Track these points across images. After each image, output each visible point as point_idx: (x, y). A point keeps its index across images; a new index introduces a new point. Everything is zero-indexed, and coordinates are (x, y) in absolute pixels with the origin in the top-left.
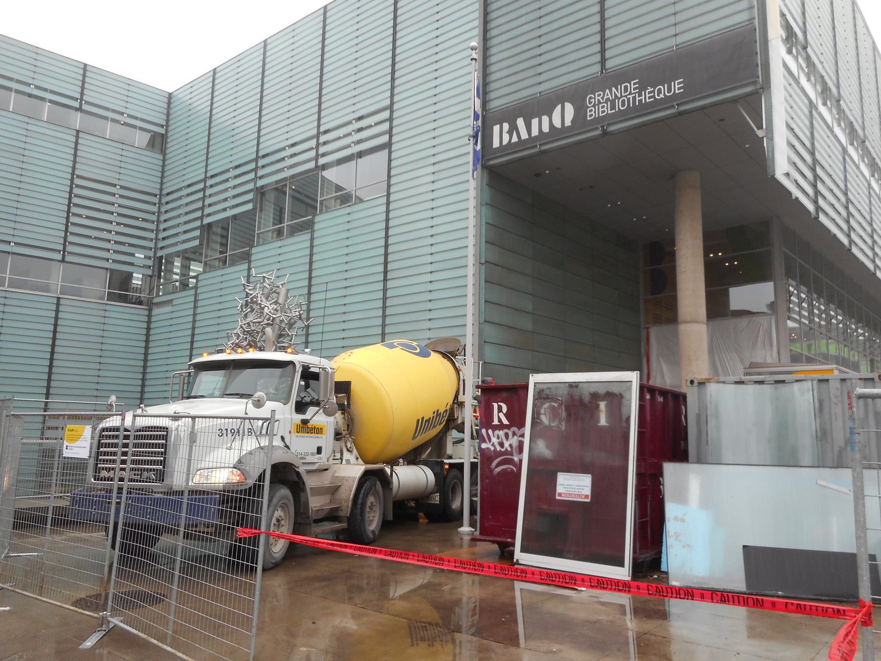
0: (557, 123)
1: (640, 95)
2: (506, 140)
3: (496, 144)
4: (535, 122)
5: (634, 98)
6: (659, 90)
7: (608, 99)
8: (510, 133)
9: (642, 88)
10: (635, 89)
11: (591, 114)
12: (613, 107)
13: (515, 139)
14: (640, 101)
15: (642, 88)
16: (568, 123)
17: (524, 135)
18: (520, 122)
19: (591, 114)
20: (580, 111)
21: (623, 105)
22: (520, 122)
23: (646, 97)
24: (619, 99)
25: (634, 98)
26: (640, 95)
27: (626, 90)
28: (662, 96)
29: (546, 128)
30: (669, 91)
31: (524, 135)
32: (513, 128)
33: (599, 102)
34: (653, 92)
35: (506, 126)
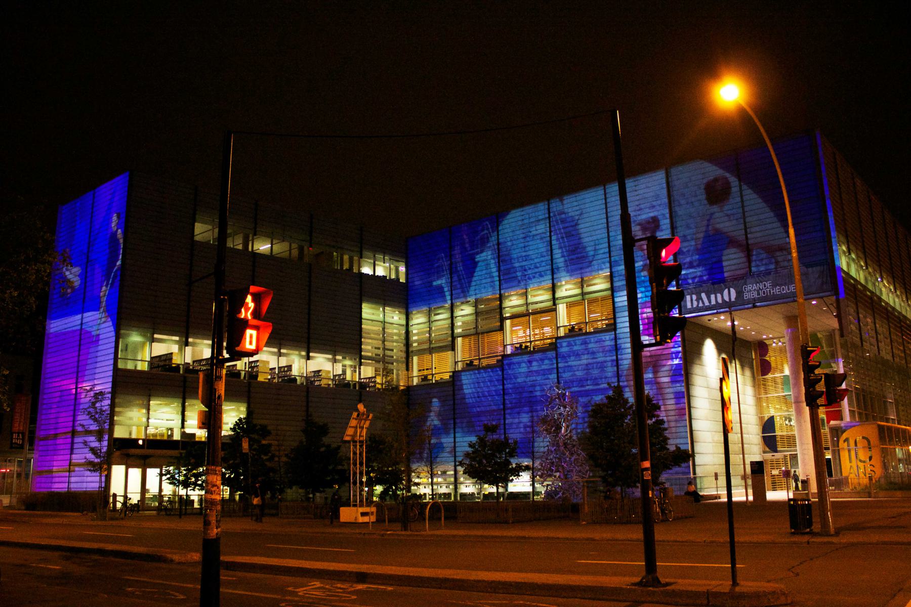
0: (727, 299)
1: (773, 290)
2: (695, 306)
3: (689, 305)
4: (713, 297)
5: (770, 291)
6: (783, 288)
7: (755, 289)
8: (697, 300)
9: (774, 286)
10: (770, 286)
11: (747, 296)
12: (759, 294)
13: (701, 305)
14: (773, 293)
15: (774, 286)
16: (733, 299)
17: (707, 303)
18: (703, 295)
19: (747, 296)
20: (739, 294)
21: (764, 293)
22: (703, 295)
23: (777, 290)
24: (762, 290)
25: (770, 291)
26: (773, 290)
27: (765, 286)
28: (785, 292)
29: (720, 301)
30: (789, 289)
31: (707, 303)
32: (699, 299)
33: (750, 291)
34: (780, 289)
35: (694, 297)
